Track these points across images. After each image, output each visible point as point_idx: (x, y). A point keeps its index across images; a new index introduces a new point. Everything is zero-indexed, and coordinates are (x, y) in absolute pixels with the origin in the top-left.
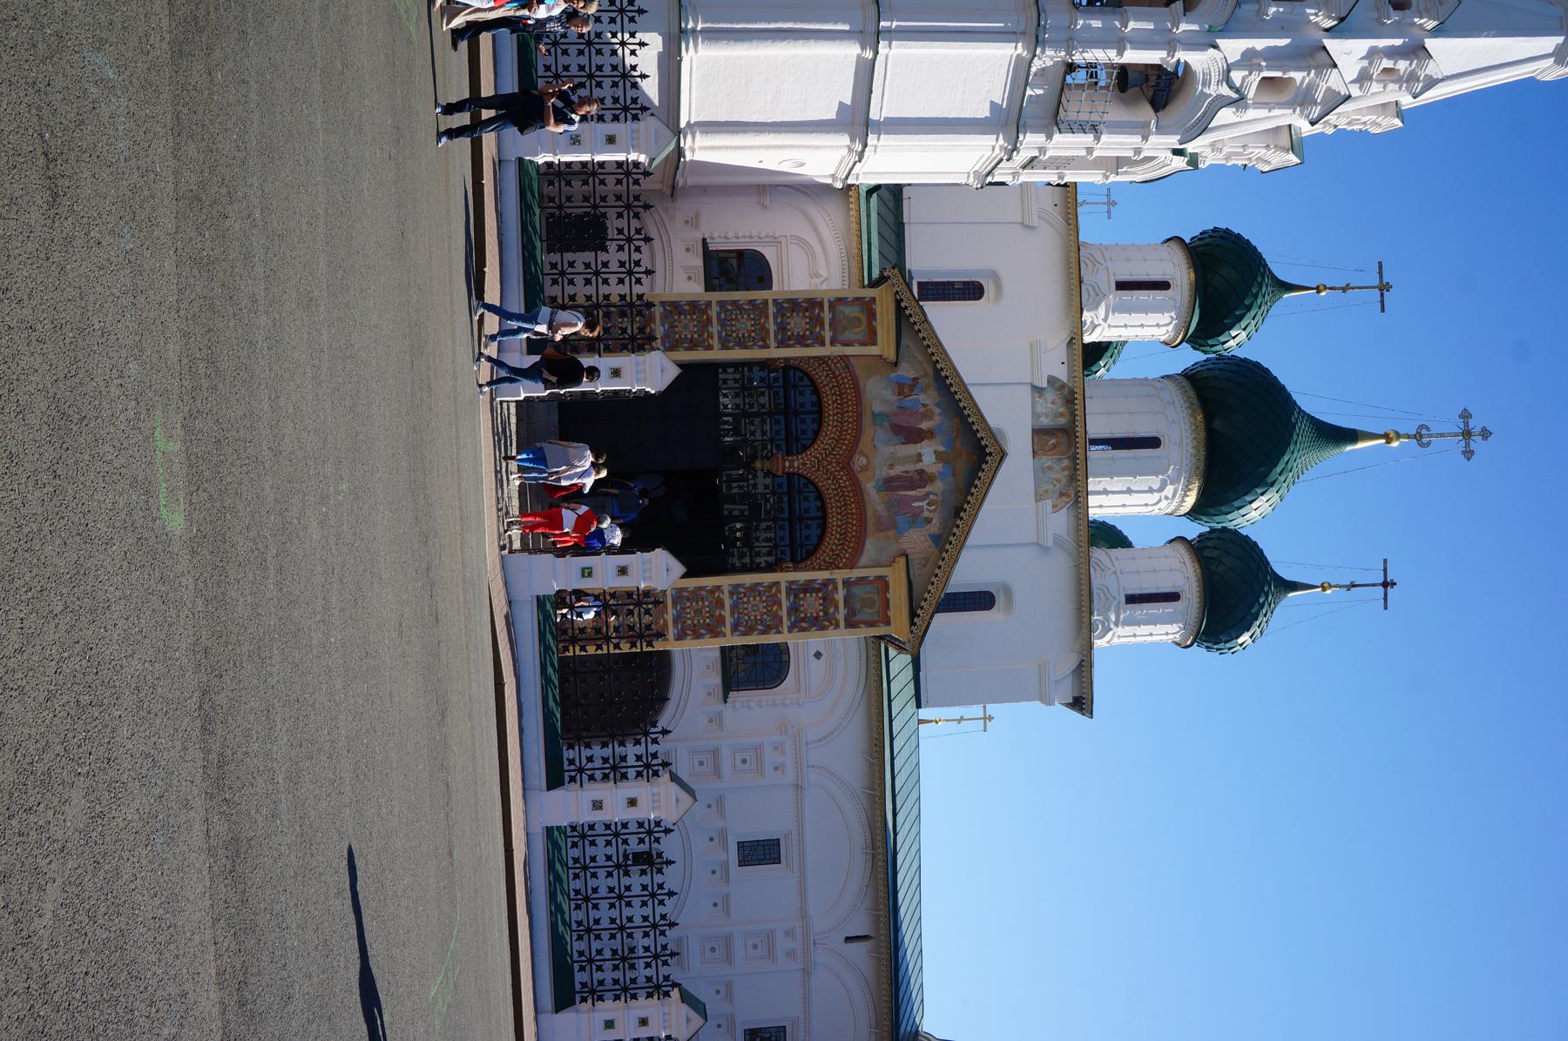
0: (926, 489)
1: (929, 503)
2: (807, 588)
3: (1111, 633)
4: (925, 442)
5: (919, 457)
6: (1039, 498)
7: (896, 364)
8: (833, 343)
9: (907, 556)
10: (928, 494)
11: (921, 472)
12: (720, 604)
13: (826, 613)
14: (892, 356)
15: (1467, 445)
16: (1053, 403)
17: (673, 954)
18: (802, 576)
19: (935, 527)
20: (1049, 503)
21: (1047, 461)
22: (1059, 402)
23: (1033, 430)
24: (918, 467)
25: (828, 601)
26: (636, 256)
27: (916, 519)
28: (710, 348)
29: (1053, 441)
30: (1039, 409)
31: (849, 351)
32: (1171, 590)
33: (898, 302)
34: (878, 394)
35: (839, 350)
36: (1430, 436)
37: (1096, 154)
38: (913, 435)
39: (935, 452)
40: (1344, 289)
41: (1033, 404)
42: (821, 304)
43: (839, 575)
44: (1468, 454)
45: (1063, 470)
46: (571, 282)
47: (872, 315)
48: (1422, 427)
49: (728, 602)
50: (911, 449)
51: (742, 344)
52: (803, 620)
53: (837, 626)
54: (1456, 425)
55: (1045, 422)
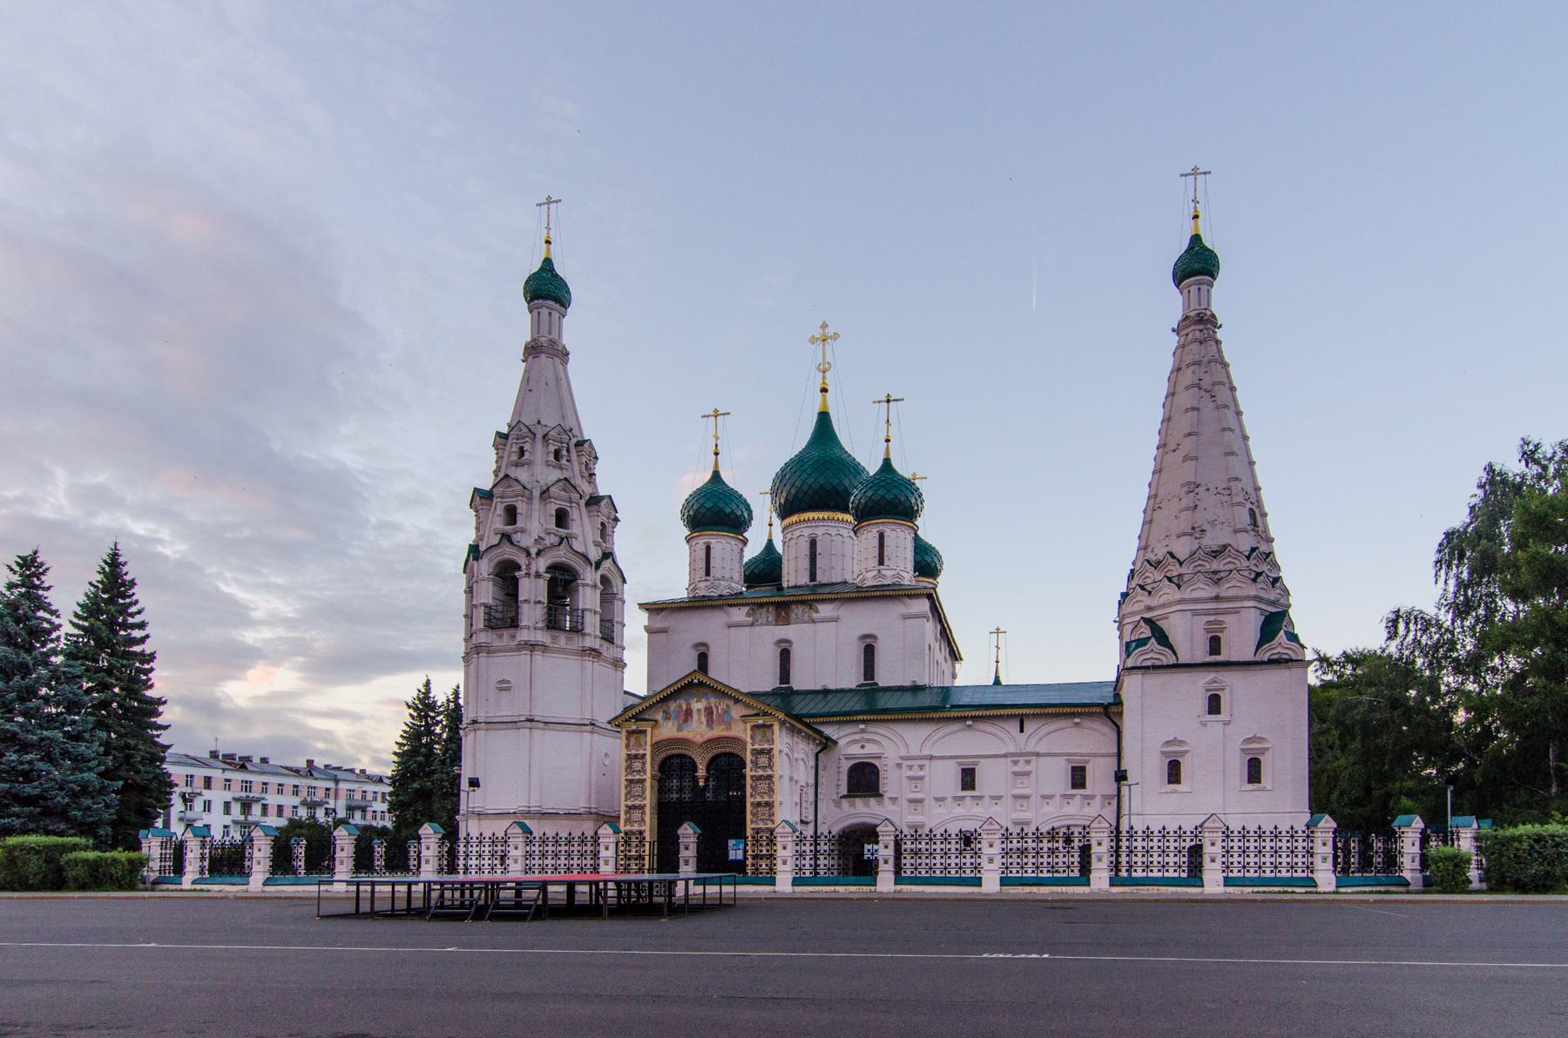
0: (713, 705)
1: (720, 705)
2: (755, 763)
3: (901, 573)
5: (699, 710)
7: (656, 721)
8: (645, 750)
9: (743, 716)
10: (715, 706)
11: (706, 709)
12: (759, 804)
13: (767, 753)
14: (653, 723)
16: (761, 614)
17: (916, 831)
18: (749, 765)
19: (731, 703)
20: (815, 615)
22: (760, 611)
23: (776, 625)
24: (703, 710)
25: (762, 752)
26: (563, 839)
27: (727, 712)
28: (645, 805)
30: (765, 622)
31: (649, 743)
32: (877, 540)
33: (627, 720)
34: (668, 730)
35: (649, 748)
37: (598, 609)
38: (689, 713)
39: (697, 702)
40: (717, 438)
41: (762, 625)
42: (628, 755)
43: (749, 747)
44: (836, 336)
45: (797, 608)
46: (572, 865)
47: (634, 732)
49: (759, 799)
50: (695, 716)
51: (643, 792)
52: (770, 765)
53: (772, 749)
54: (820, 346)
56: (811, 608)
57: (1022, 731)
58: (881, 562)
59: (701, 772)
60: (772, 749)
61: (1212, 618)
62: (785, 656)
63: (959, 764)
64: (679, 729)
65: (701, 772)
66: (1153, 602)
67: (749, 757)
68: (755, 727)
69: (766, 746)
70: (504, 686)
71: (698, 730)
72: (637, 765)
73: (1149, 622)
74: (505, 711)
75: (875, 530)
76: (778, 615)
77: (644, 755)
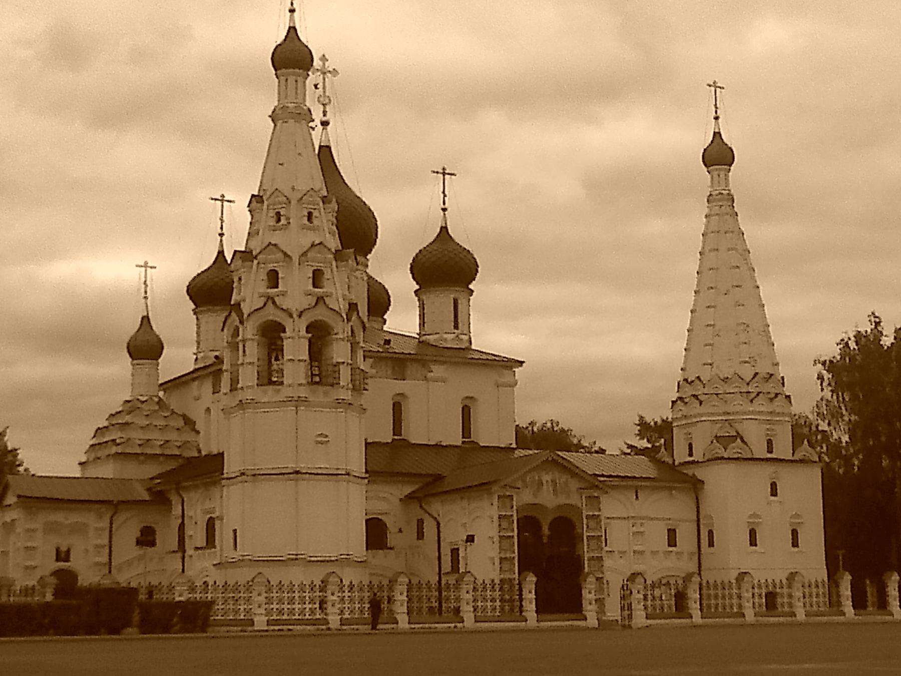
4: (542, 478)
5: (547, 481)
6: (425, 378)
15: (324, 64)
20: (430, 375)
21: (409, 372)
28: (514, 558)
29: (396, 368)
36: (325, 96)
39: (546, 474)
42: (500, 515)
43: (585, 513)
48: (319, 101)
49: (592, 555)
50: (545, 487)
55: (389, 372)
56: (424, 366)
57: (637, 497)
58: (456, 327)
59: (546, 531)
60: (599, 516)
61: (768, 427)
62: (397, 408)
63: (666, 524)
64: (535, 495)
65: (546, 531)
66: (730, 409)
67: (585, 521)
68: (587, 498)
69: (596, 513)
70: (322, 440)
71: (549, 499)
72: (505, 524)
73: (730, 423)
74: (322, 464)
75: (452, 296)
76: (394, 368)
77: (512, 516)
